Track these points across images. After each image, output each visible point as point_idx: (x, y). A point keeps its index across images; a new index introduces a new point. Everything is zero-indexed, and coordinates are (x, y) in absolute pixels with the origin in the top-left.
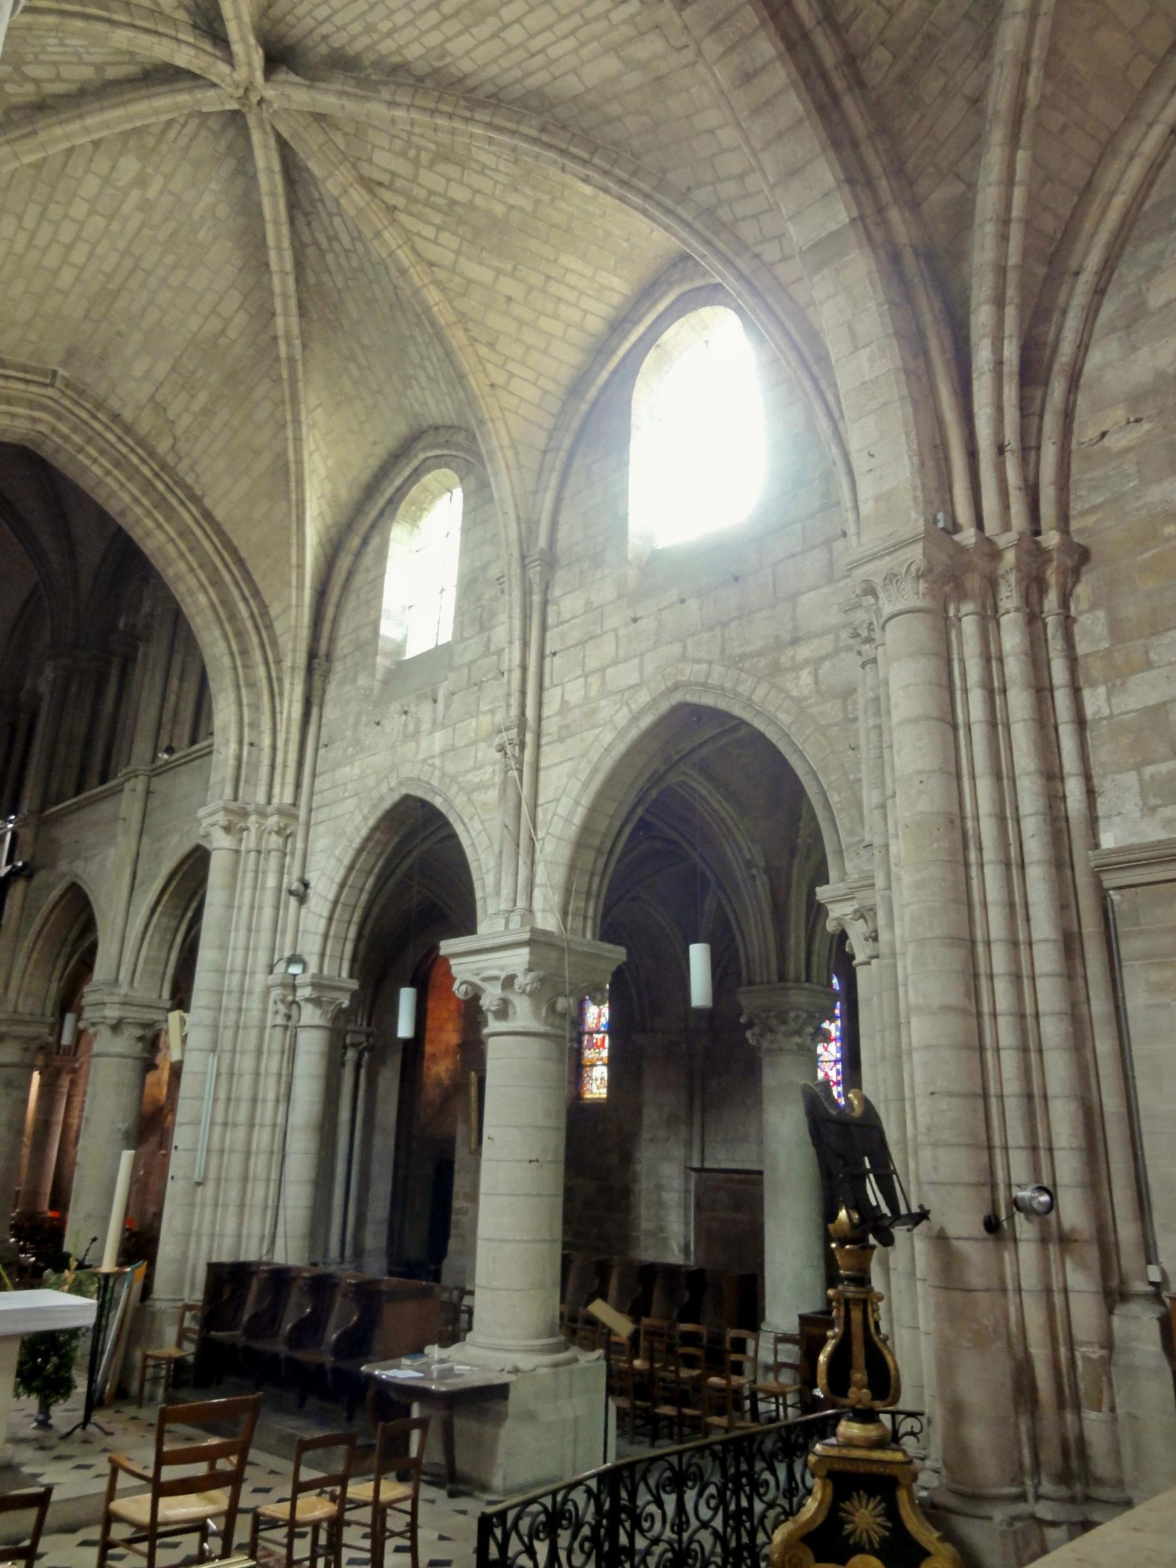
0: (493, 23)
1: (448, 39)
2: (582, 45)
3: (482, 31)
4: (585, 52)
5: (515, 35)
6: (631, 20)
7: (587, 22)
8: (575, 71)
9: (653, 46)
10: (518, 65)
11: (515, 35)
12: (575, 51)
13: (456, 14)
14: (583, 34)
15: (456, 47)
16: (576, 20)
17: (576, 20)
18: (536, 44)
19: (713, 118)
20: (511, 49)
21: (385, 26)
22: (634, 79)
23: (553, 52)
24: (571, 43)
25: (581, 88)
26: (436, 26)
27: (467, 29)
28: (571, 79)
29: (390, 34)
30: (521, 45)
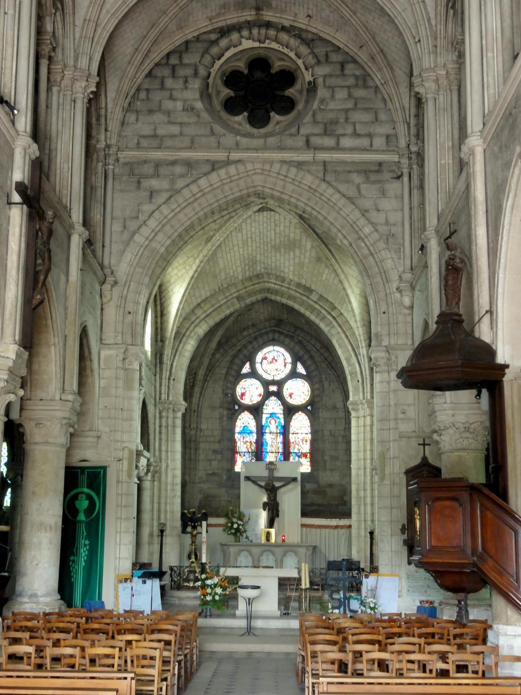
0: (241, 246)
1: (242, 235)
2: (228, 261)
3: (240, 243)
4: (226, 261)
5: (236, 248)
6: (229, 273)
7: (232, 264)
8: (222, 257)
9: (223, 276)
10: (229, 246)
11: (236, 248)
12: (227, 259)
13: (247, 240)
14: (230, 263)
15: (240, 235)
16: (233, 262)
17: (233, 262)
18: (232, 251)
19: (207, 288)
20: (233, 246)
21: (253, 224)
22: (217, 271)
23: (229, 255)
24: (229, 259)
25: (218, 256)
26: (247, 234)
27: (242, 240)
28: (221, 255)
29: (251, 224)
30: (233, 249)
